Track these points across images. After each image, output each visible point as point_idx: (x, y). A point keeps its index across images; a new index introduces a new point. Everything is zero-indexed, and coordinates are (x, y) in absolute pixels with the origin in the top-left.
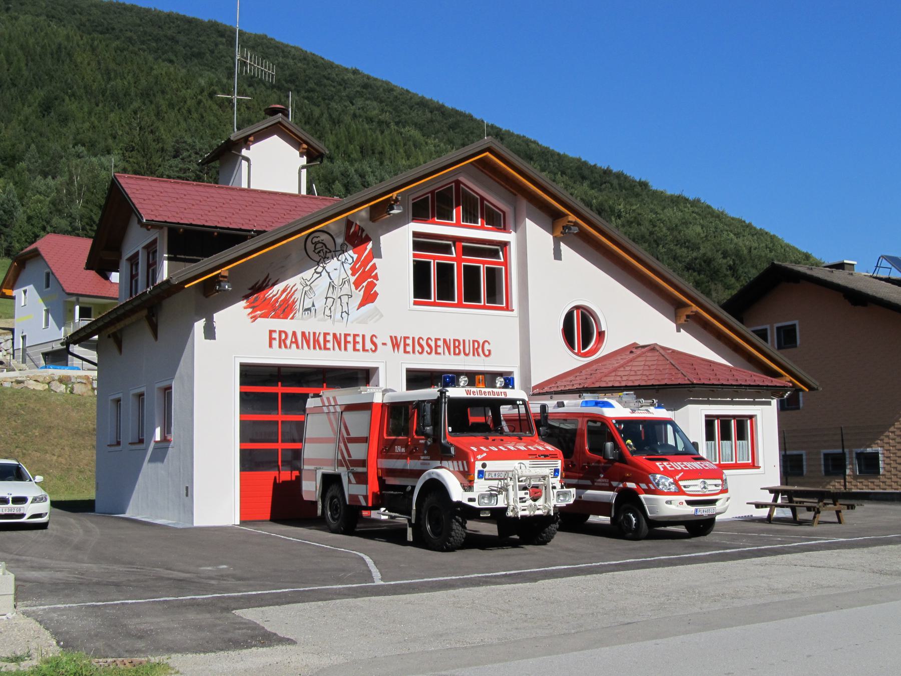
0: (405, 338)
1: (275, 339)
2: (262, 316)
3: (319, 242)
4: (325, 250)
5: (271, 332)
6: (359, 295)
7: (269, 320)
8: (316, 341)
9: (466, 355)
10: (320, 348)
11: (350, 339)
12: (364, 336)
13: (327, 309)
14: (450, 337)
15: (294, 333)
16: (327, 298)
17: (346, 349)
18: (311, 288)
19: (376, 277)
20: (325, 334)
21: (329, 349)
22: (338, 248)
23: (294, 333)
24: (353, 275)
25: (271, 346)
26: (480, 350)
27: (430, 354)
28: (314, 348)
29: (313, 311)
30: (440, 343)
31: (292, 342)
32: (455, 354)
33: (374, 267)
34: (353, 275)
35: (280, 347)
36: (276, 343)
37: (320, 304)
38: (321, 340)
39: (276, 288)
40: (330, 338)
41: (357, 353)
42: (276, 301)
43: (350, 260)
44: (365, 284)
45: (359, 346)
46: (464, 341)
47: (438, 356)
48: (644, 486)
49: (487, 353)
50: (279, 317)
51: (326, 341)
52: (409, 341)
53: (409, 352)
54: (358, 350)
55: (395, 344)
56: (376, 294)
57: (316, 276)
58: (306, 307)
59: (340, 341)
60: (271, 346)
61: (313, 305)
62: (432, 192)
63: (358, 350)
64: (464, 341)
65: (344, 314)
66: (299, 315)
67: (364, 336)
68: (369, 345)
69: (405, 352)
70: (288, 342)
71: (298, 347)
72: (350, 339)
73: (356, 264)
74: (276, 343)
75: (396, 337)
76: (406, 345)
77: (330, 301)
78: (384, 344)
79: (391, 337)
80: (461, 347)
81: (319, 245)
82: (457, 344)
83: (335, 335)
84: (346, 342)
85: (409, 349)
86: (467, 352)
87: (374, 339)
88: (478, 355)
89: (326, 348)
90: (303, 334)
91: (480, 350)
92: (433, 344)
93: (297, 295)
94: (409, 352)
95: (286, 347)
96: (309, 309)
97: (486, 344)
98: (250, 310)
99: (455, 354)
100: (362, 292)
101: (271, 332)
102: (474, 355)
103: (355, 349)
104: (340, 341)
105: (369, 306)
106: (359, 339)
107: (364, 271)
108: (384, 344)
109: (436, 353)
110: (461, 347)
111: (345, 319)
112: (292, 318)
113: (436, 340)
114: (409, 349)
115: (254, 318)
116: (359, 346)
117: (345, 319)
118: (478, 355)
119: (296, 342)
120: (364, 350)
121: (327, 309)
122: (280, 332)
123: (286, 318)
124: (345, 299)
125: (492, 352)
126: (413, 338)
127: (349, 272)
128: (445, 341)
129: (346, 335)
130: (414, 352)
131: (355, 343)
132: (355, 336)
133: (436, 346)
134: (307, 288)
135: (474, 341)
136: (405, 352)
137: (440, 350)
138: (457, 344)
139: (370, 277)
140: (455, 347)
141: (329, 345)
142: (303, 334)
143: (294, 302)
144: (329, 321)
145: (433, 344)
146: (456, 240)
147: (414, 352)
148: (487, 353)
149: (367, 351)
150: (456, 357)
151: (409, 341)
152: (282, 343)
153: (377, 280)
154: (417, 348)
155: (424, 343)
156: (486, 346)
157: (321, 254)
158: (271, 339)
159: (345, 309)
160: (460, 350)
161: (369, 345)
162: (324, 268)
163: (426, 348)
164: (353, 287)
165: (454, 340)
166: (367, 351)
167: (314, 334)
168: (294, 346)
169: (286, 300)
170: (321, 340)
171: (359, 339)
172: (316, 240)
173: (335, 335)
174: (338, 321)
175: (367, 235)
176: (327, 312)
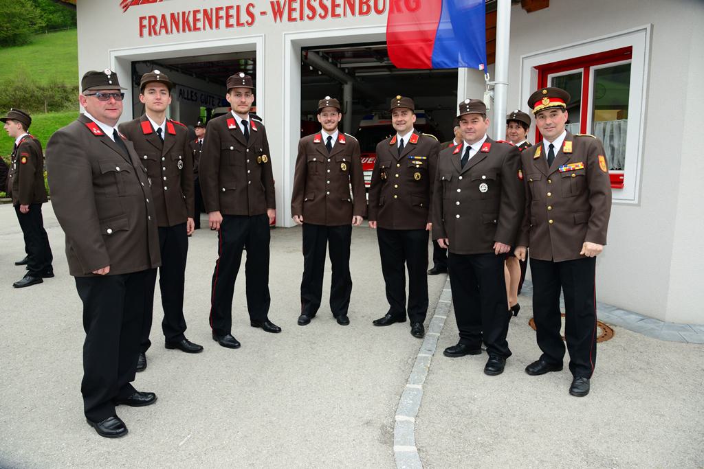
5: (141, 19)
7: (140, 6)
8: (186, 22)
10: (190, 30)
11: (222, 13)
12: (238, 7)
15: (163, 16)
17: (217, 26)
20: (196, 12)
21: (199, 29)
23: (163, 16)
25: (141, 35)
28: (184, 30)
31: (161, 27)
32: (361, 13)
35: (150, 34)
36: (146, 31)
38: (191, 19)
40: (200, 16)
45: (233, 21)
47: (336, 19)
51: (196, 20)
53: (295, 19)
54: (232, 26)
59: (211, 18)
60: (141, 35)
63: (232, 26)
67: (238, 7)
68: (245, 18)
69: (291, 19)
70: (158, 28)
71: (167, 32)
74: (146, 31)
78: (263, 13)
80: (372, 3)
83: (205, 11)
84: (218, 18)
85: (296, 15)
86: (381, 8)
87: (251, 8)
89: (196, 29)
94: (295, 19)
95: (155, 33)
101: (141, 19)
103: (228, 25)
104: (211, 18)
106: (233, 12)
108: (263, 13)
109: (334, 15)
114: (296, 15)
116: (233, 21)
119: (165, 27)
120: (239, 24)
122: (150, 17)
129: (218, 9)
130: (302, 18)
131: (228, 17)
132: (228, 8)
136: (291, 19)
141: (199, 25)
142: (172, 16)
147: (302, 18)
149: (243, 24)
150: (364, 17)
152: (153, 30)
154: (307, 12)
158: (142, 27)
160: (369, 7)
161: (245, 18)
163: (320, 11)
166: (243, 24)
167: (184, 13)
168: (163, 31)
170: (191, 19)
171: (233, 12)
173: (205, 11)
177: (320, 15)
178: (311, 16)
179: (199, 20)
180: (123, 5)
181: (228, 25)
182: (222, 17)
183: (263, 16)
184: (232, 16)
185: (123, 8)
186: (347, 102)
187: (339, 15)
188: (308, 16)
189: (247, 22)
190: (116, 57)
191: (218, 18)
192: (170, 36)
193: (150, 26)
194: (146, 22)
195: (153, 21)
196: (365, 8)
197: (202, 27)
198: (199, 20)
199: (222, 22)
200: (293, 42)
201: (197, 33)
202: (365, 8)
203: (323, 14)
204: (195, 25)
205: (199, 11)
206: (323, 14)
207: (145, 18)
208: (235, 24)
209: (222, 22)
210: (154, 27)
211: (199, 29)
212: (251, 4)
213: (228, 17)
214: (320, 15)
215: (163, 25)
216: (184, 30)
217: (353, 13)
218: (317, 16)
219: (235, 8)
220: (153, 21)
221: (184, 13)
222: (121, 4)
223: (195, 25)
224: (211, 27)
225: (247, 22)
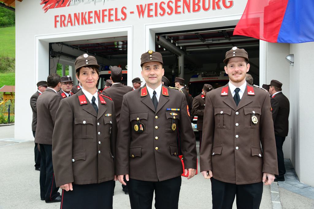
0: (149, 5)
1: (58, 21)
2: (50, 8)
5: (56, 17)
8: (84, 18)
9: (205, 9)
10: (86, 23)
11: (106, 13)
12: (116, 9)
15: (70, 16)
17: (103, 21)
20: (90, 13)
21: (92, 23)
23: (70, 16)
25: (56, 26)
28: (82, 24)
31: (68, 22)
32: (194, 11)
35: (61, 26)
36: (58, 24)
40: (92, 15)
41: (111, 23)
45: (113, 18)
49: (228, 4)
50: (60, 6)
51: (90, 17)
52: (152, 7)
53: (152, 16)
55: (141, 10)
59: (99, 16)
60: (56, 26)
67: (116, 9)
68: (120, 15)
69: (149, 16)
70: (66, 22)
71: (72, 25)
74: (58, 24)
75: (141, 6)
76: (149, 10)
78: (132, 13)
79: (137, 6)
80: (201, 4)
83: (96, 12)
84: (104, 16)
85: (153, 13)
86: (207, 6)
87: (124, 10)
88: (219, 7)
89: (90, 23)
94: (152, 16)
95: (64, 26)
98: (44, 5)
99: (194, 11)
101: (56, 17)
102: (214, 8)
103: (110, 20)
104: (99, 16)
106: (113, 12)
108: (132, 13)
109: (177, 12)
112: (69, 5)
115: (46, 10)
116: (113, 18)
118: (219, 7)
119: (71, 22)
120: (117, 19)
122: (61, 16)
123: (65, 6)
125: (234, 3)
126: (156, 4)
129: (104, 11)
130: (156, 15)
131: (110, 15)
132: (110, 10)
133: (177, 7)
136: (149, 16)
137: (180, 10)
141: (92, 20)
142: (75, 15)
147: (156, 15)
148: (228, 4)
149: (119, 20)
151: (152, 7)
152: (63, 24)
154: (160, 11)
155: (165, 6)
158: (56, 21)
161: (120, 15)
163: (167, 10)
166: (119, 20)
167: (82, 13)
168: (69, 24)
171: (113, 12)
173: (96, 12)
177: (168, 13)
178: (162, 13)
179: (92, 17)
180: (44, 8)
181: (110, 20)
182: (106, 16)
183: (132, 15)
184: (112, 15)
185: (45, 10)
186: (181, 67)
187: (180, 13)
188: (160, 14)
189: (122, 18)
190: (40, 40)
191: (104, 16)
192: (73, 27)
193: (61, 21)
194: (58, 19)
196: (197, 8)
197: (93, 22)
198: (92, 17)
199: (106, 19)
200: (151, 30)
201: (90, 25)
202: (197, 8)
203: (170, 12)
205: (91, 12)
206: (170, 12)
207: (58, 16)
208: (114, 19)
209: (106, 19)
210: (64, 22)
211: (92, 23)
214: (168, 13)
215: (69, 20)
216: (82, 24)
217: (189, 11)
218: (166, 14)
219: (114, 10)
222: (43, 8)
224: (99, 22)
225: (122, 18)
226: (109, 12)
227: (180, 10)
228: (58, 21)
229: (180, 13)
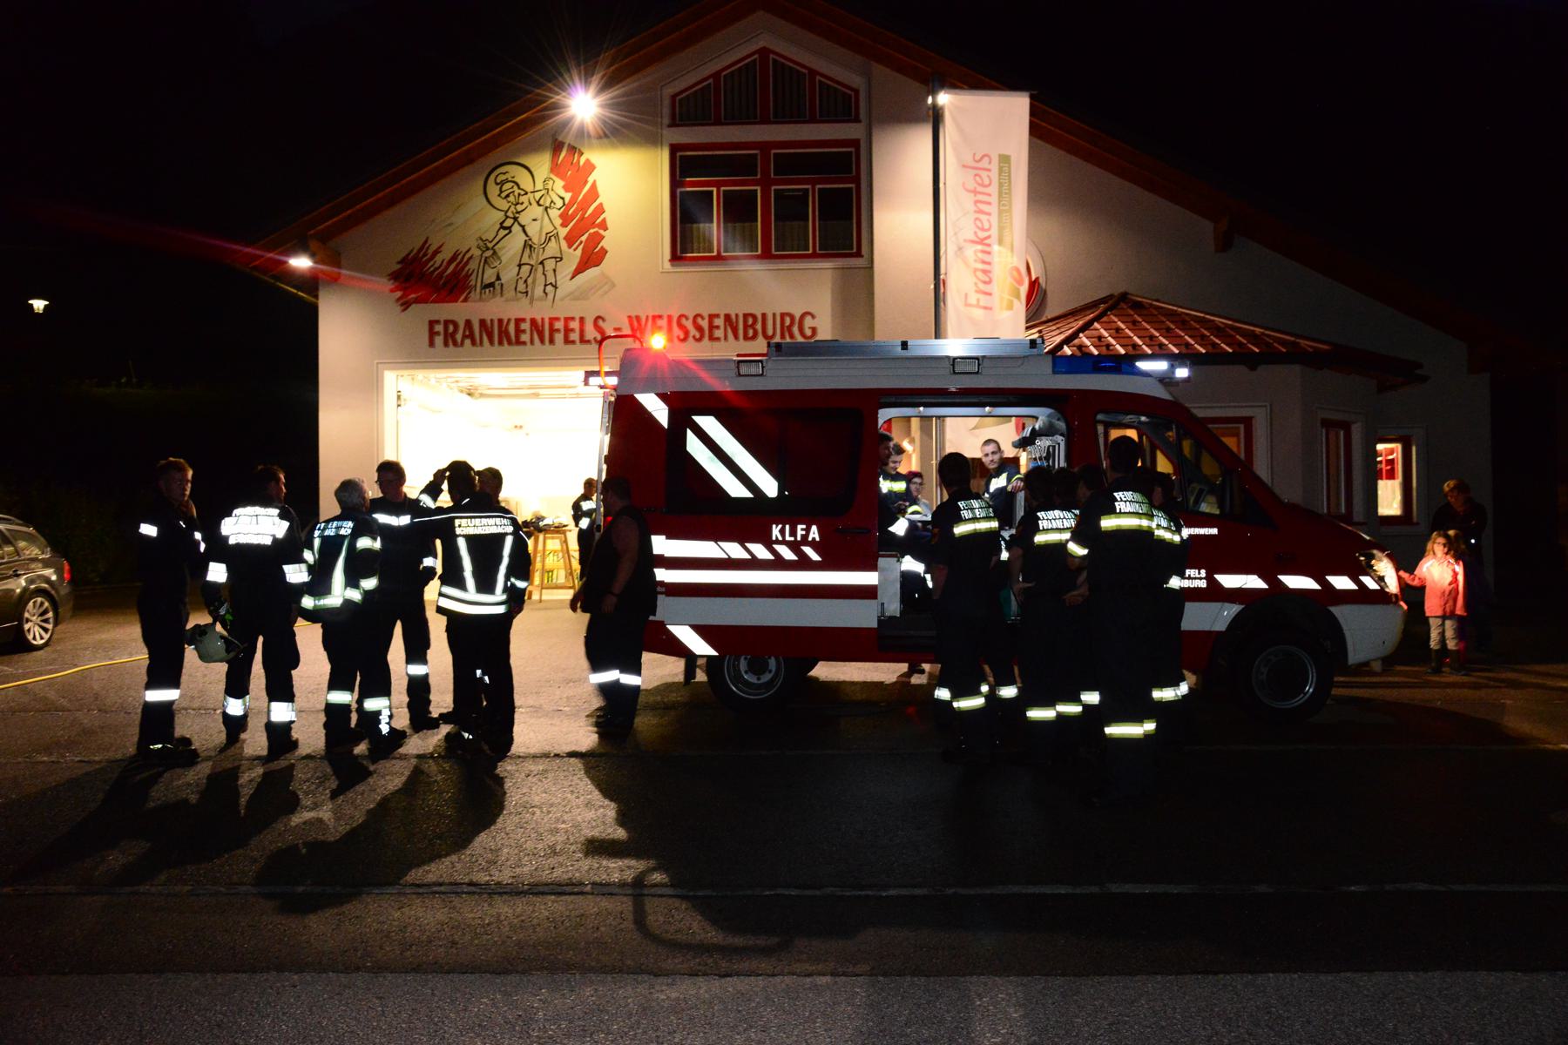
1: (438, 333)
2: (417, 301)
3: (507, 181)
4: (517, 191)
5: (432, 323)
6: (574, 256)
8: (504, 333)
10: (510, 343)
11: (559, 325)
12: (582, 319)
13: (521, 283)
14: (737, 309)
15: (468, 323)
16: (520, 266)
17: (552, 341)
18: (495, 253)
19: (604, 226)
20: (519, 321)
22: (539, 186)
23: (468, 323)
24: (564, 225)
25: (432, 344)
26: (795, 329)
27: (699, 340)
28: (501, 343)
29: (498, 287)
30: (719, 322)
31: (464, 337)
33: (600, 210)
34: (564, 225)
35: (446, 344)
36: (439, 340)
37: (509, 275)
39: (439, 258)
40: (526, 326)
42: (440, 276)
43: (559, 203)
44: (584, 238)
45: (575, 336)
46: (764, 315)
48: (1342, 583)
51: (519, 331)
54: (573, 342)
56: (604, 252)
57: (503, 232)
58: (487, 281)
60: (432, 344)
61: (498, 278)
62: (716, 75)
63: (573, 342)
64: (764, 315)
65: (549, 288)
66: (475, 295)
67: (582, 319)
68: (591, 333)
70: (459, 337)
71: (474, 343)
72: (559, 325)
73: (567, 206)
74: (439, 340)
75: (638, 318)
77: (526, 269)
80: (759, 327)
81: (508, 185)
82: (750, 321)
83: (533, 321)
87: (600, 323)
89: (519, 342)
90: (483, 322)
91: (795, 329)
92: (705, 324)
93: (473, 265)
95: (455, 344)
96: (491, 285)
97: (808, 320)
98: (399, 294)
100: (579, 252)
103: (567, 341)
105: (592, 273)
106: (575, 325)
107: (582, 218)
109: (712, 338)
110: (759, 327)
111: (550, 296)
112: (465, 300)
113: (712, 317)
115: (406, 305)
116: (575, 336)
117: (550, 296)
119: (471, 336)
120: (583, 341)
121: (521, 283)
122: (447, 323)
124: (550, 264)
126: (670, 317)
127: (558, 222)
128: (727, 317)
129: (553, 320)
131: (568, 331)
132: (567, 320)
133: (712, 327)
134: (488, 253)
135: (783, 315)
137: (719, 333)
138: (750, 321)
139: (593, 225)
140: (746, 327)
141: (525, 337)
142: (483, 322)
143: (468, 276)
144: (525, 301)
145: (705, 324)
146: (765, 147)
149: (588, 342)
153: (606, 229)
155: (689, 324)
156: (808, 322)
157: (511, 198)
158: (432, 334)
159: (551, 279)
161: (591, 333)
162: (515, 219)
163: (693, 332)
164: (564, 244)
165: (746, 316)
166: (588, 342)
167: (500, 321)
168: (468, 342)
169: (454, 273)
171: (575, 325)
172: (502, 178)
174: (540, 299)
175: (587, 161)
176: (521, 287)
181: (567, 341)
187: (718, 339)
191: (553, 331)
194: (439, 328)
195: (451, 328)
196: (751, 333)
199: (559, 337)
202: (751, 333)
204: (517, 336)
209: (559, 337)
212: (599, 317)
213: (568, 331)
217: (736, 337)
218: (691, 339)
220: (451, 328)
221: (500, 321)
223: (517, 336)
224: (542, 341)
226: (566, 327)
227: (719, 333)
228: (438, 333)
229: (718, 339)
